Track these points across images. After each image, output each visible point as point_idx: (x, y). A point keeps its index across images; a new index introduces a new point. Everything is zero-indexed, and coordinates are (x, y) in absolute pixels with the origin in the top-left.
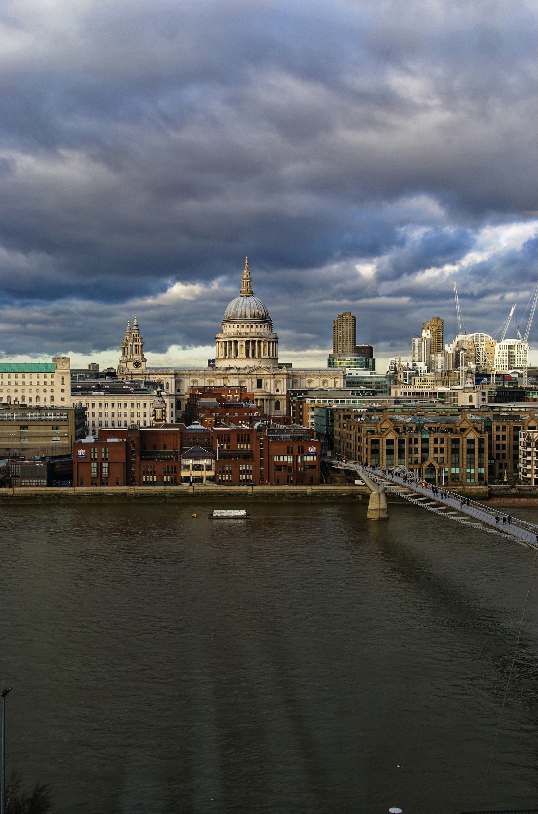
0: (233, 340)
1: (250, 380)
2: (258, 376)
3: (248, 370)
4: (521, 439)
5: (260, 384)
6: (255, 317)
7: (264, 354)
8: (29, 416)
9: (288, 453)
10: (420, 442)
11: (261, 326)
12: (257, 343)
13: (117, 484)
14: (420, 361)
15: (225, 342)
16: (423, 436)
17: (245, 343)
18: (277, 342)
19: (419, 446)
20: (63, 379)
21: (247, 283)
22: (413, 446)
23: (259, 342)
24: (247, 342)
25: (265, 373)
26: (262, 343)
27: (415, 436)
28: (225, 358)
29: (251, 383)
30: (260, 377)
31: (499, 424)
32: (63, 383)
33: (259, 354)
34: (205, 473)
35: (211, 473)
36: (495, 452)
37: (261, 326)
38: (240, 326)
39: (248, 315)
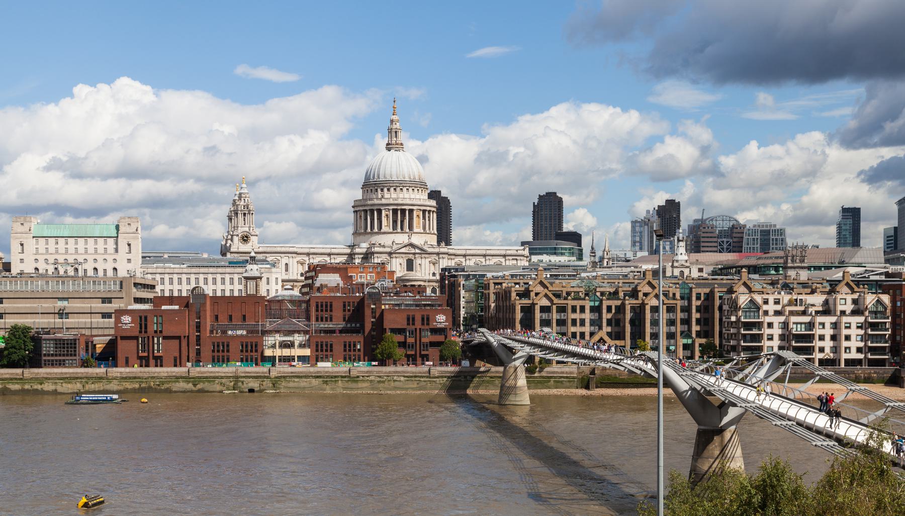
0: (375, 208)
3: (395, 247)
4: (726, 307)
5: (410, 266)
8: (70, 287)
9: (408, 324)
10: (587, 310)
13: (175, 366)
14: (641, 249)
15: (366, 211)
16: (592, 304)
19: (587, 316)
20: (129, 245)
22: (577, 316)
24: (395, 212)
25: (417, 251)
26: (415, 213)
27: (581, 303)
28: (365, 233)
30: (411, 256)
31: (700, 290)
32: (130, 252)
33: (411, 227)
34: (297, 352)
35: (307, 352)
36: (695, 328)
38: (385, 190)
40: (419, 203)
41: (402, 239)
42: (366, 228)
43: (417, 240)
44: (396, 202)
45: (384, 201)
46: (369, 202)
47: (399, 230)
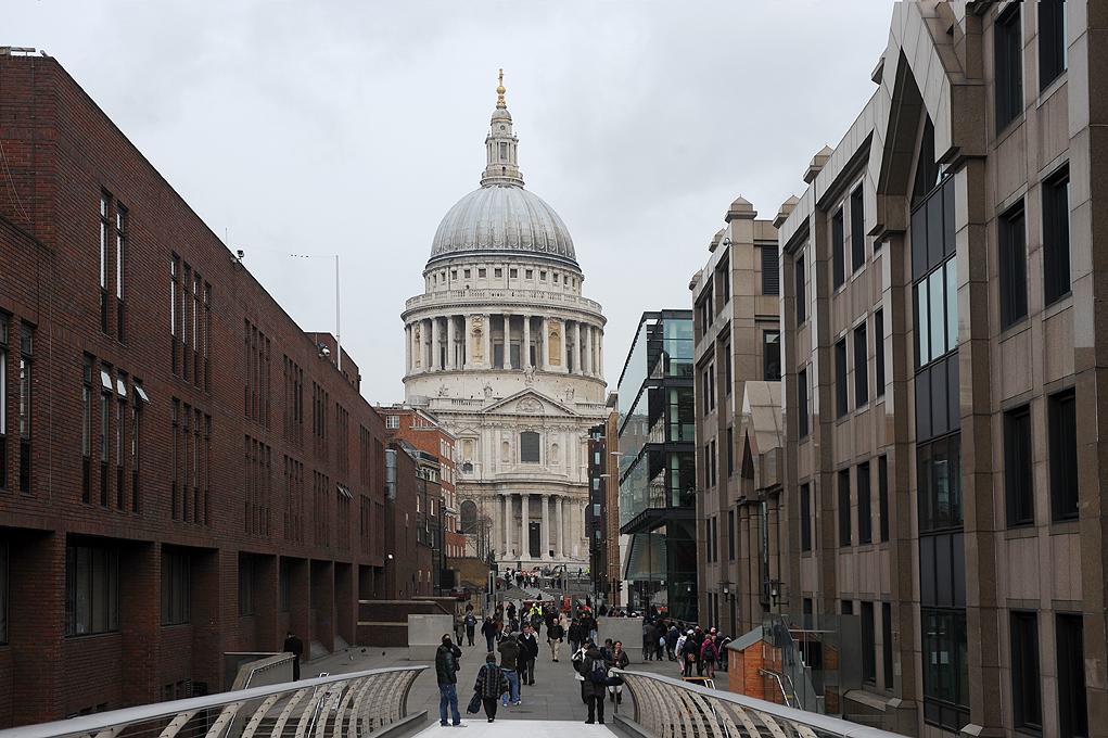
0: (448, 313)
1: (498, 432)
2: (522, 421)
3: (489, 403)
5: (530, 450)
6: (522, 243)
7: (555, 361)
11: (543, 274)
12: (527, 324)
15: (428, 322)
17: (487, 322)
18: (602, 332)
21: (504, 145)
23: (536, 322)
24: (497, 321)
26: (546, 325)
29: (498, 443)
30: (531, 424)
37: (543, 274)
38: (475, 272)
39: (499, 235)
40: (556, 303)
41: (507, 386)
42: (431, 365)
43: (543, 387)
44: (498, 299)
45: (468, 298)
46: (433, 301)
47: (507, 366)
